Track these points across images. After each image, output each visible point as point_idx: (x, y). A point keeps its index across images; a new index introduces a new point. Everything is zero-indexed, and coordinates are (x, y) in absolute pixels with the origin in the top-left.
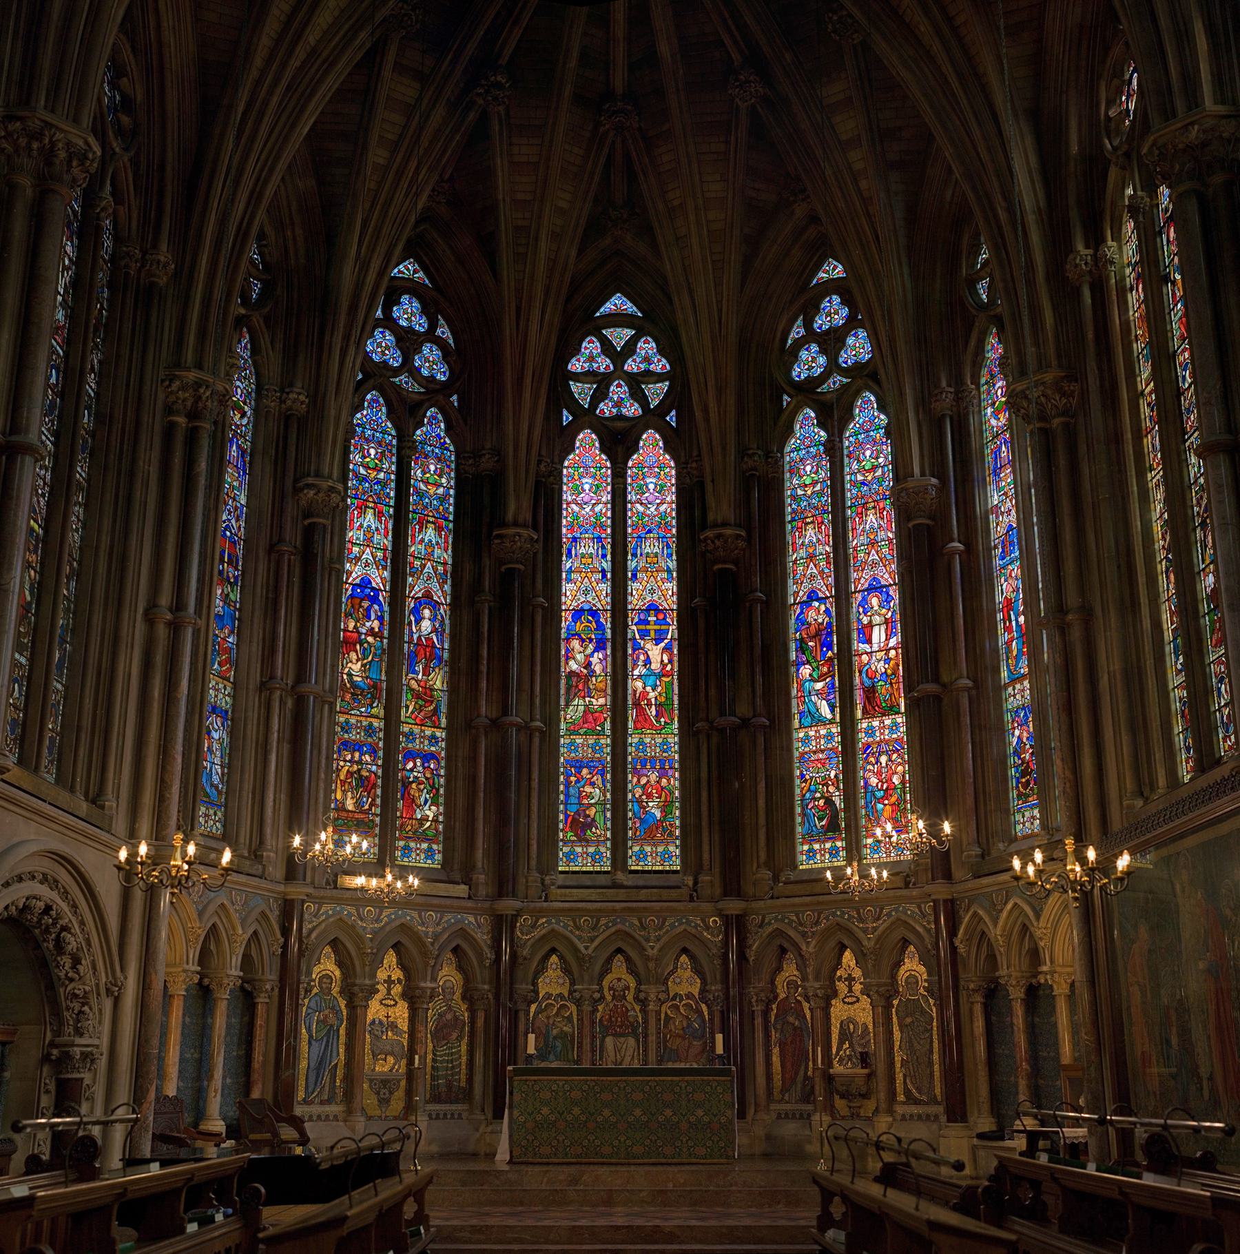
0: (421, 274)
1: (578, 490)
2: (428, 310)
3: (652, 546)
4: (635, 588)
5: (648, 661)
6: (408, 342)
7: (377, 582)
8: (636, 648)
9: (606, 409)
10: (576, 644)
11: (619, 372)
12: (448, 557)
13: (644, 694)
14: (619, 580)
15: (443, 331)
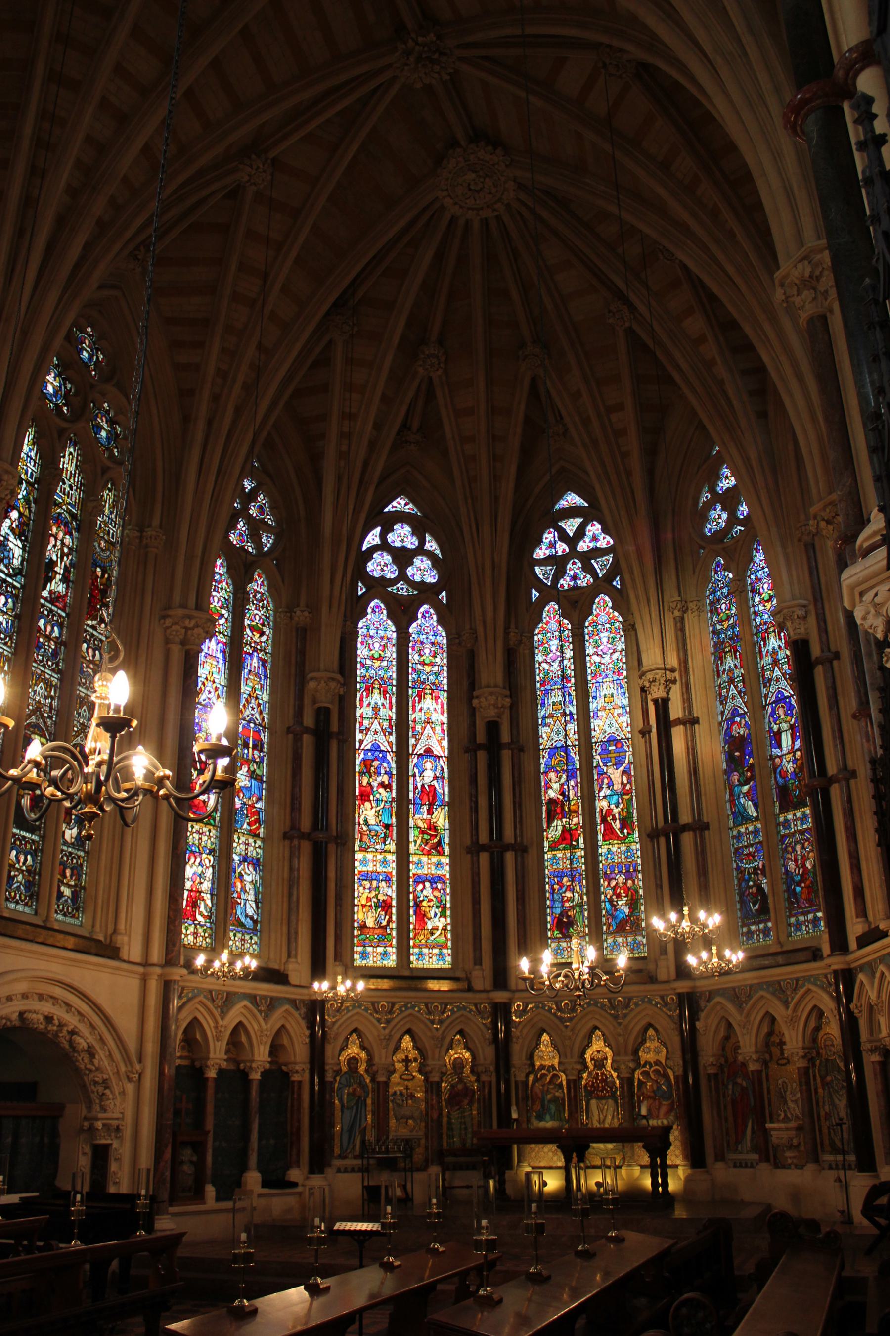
0: (411, 506)
1: (547, 652)
2: (419, 532)
3: (607, 688)
4: (595, 723)
5: (610, 785)
6: (403, 557)
7: (384, 746)
8: (601, 774)
9: (565, 583)
10: (552, 775)
11: (573, 553)
12: (444, 718)
13: (610, 811)
14: (584, 718)
15: (431, 545)
